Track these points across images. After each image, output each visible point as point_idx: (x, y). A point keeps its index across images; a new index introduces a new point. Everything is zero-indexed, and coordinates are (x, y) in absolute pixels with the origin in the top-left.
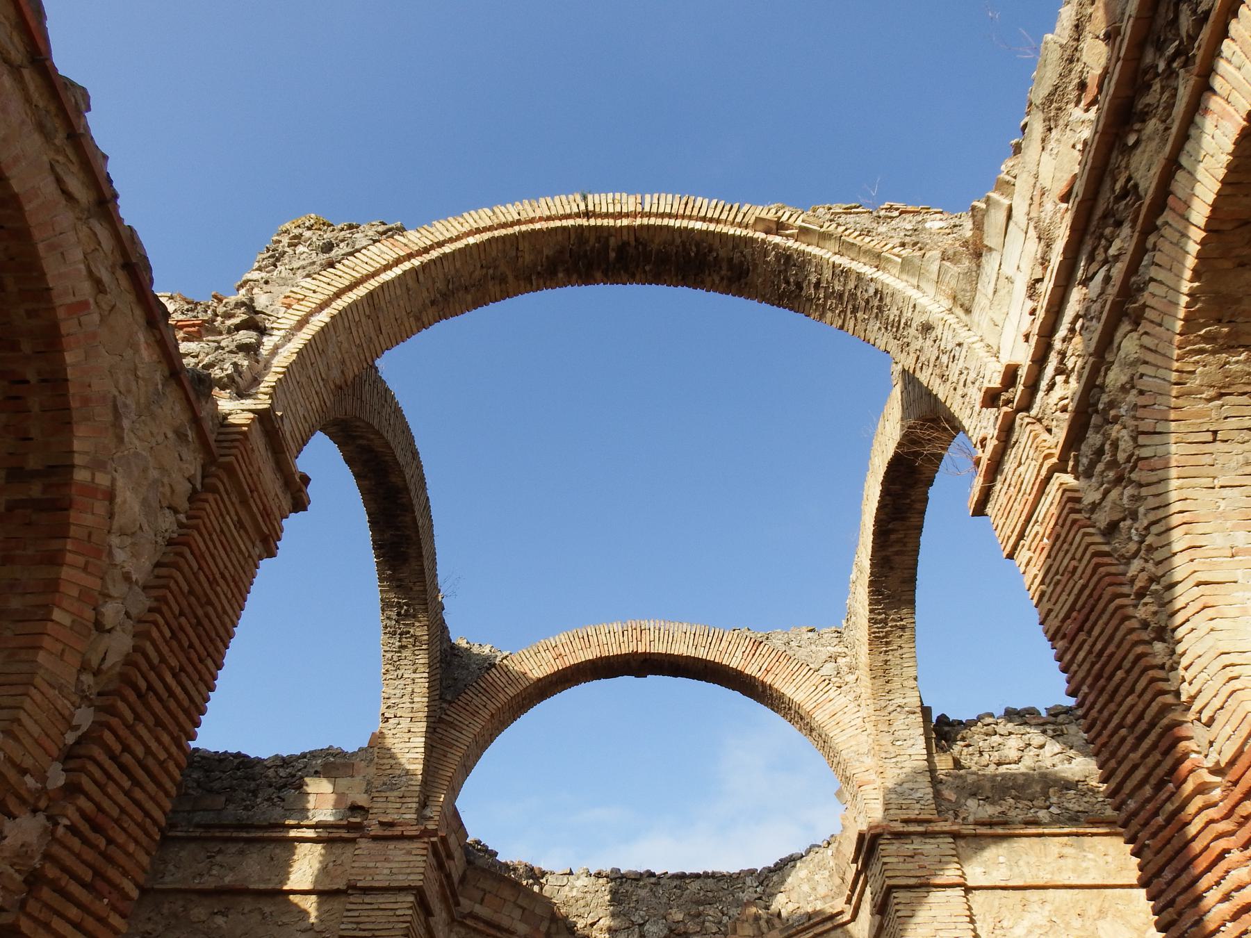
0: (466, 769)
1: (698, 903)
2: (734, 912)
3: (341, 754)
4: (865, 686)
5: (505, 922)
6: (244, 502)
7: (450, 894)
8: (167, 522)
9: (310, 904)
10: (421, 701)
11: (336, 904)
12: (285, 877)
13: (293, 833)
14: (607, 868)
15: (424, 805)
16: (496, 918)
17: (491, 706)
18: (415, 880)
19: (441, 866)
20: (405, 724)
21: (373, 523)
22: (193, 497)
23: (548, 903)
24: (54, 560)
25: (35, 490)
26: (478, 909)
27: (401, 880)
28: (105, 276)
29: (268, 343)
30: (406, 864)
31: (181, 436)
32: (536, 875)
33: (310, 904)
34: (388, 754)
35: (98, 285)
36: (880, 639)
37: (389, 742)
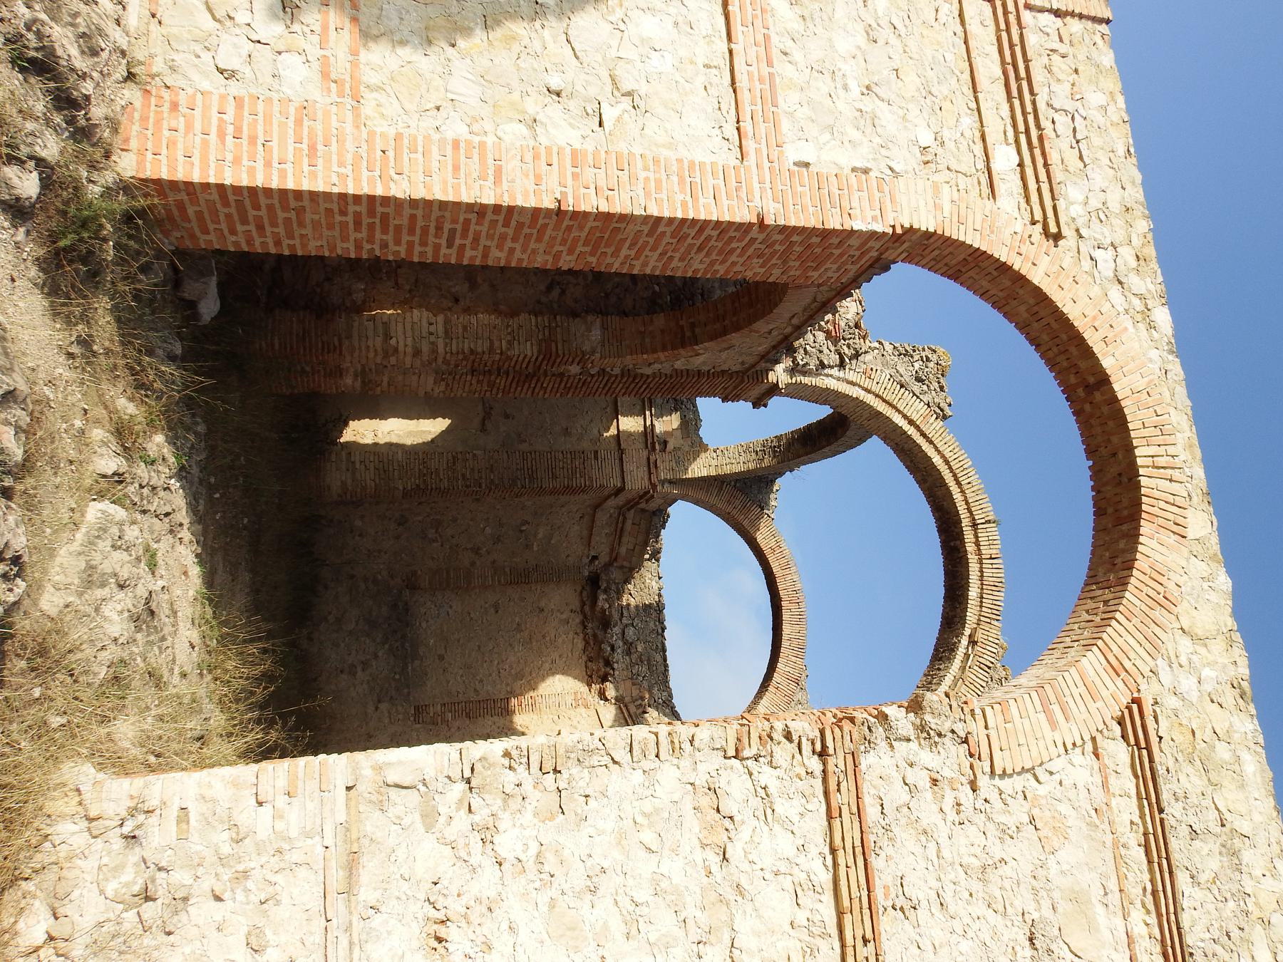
0: (697, 503)
1: (649, 660)
2: (645, 684)
3: (697, 428)
5: (625, 539)
6: (735, 388)
7: (632, 504)
9: (613, 431)
10: (727, 470)
11: (613, 444)
12: (624, 415)
13: (648, 413)
14: (665, 600)
15: (670, 482)
16: (626, 534)
17: (734, 512)
18: (628, 486)
19: (641, 497)
20: (714, 463)
21: (819, 422)
22: (723, 372)
23: (639, 565)
24: (664, 349)
25: (688, 334)
26: (629, 522)
27: (627, 478)
28: (775, 333)
29: (835, 372)
30: (637, 479)
31: (743, 363)
32: (656, 555)
33: (613, 431)
34: (696, 456)
35: (770, 333)
37: (703, 455)
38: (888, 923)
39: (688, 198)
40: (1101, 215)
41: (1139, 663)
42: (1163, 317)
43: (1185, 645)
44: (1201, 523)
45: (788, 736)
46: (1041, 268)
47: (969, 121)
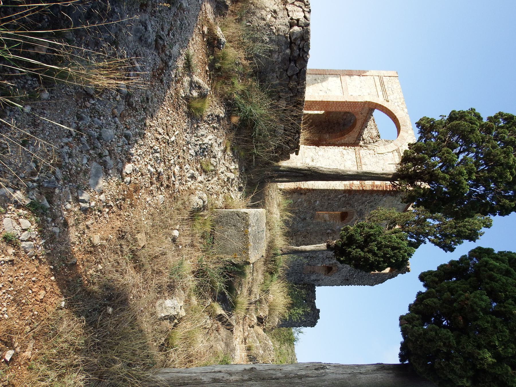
8: (347, 142)
38: (363, 166)
40: (396, 99)
42: (406, 110)
46: (385, 105)
47: (375, 90)
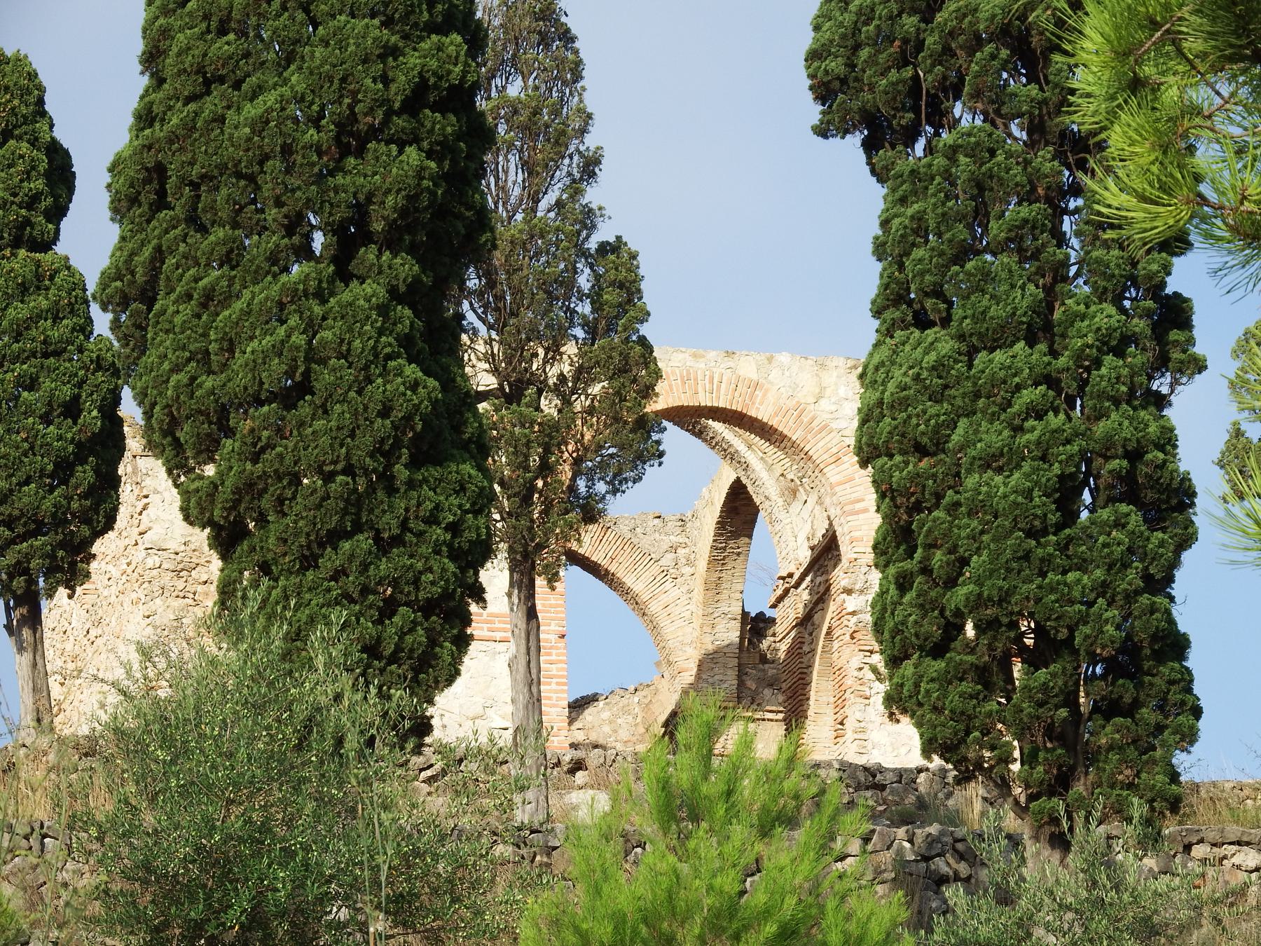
4: (699, 594)
36: (719, 560)
39: (554, 680)
41: (835, 442)
43: (824, 404)
44: (748, 367)
45: (861, 669)
